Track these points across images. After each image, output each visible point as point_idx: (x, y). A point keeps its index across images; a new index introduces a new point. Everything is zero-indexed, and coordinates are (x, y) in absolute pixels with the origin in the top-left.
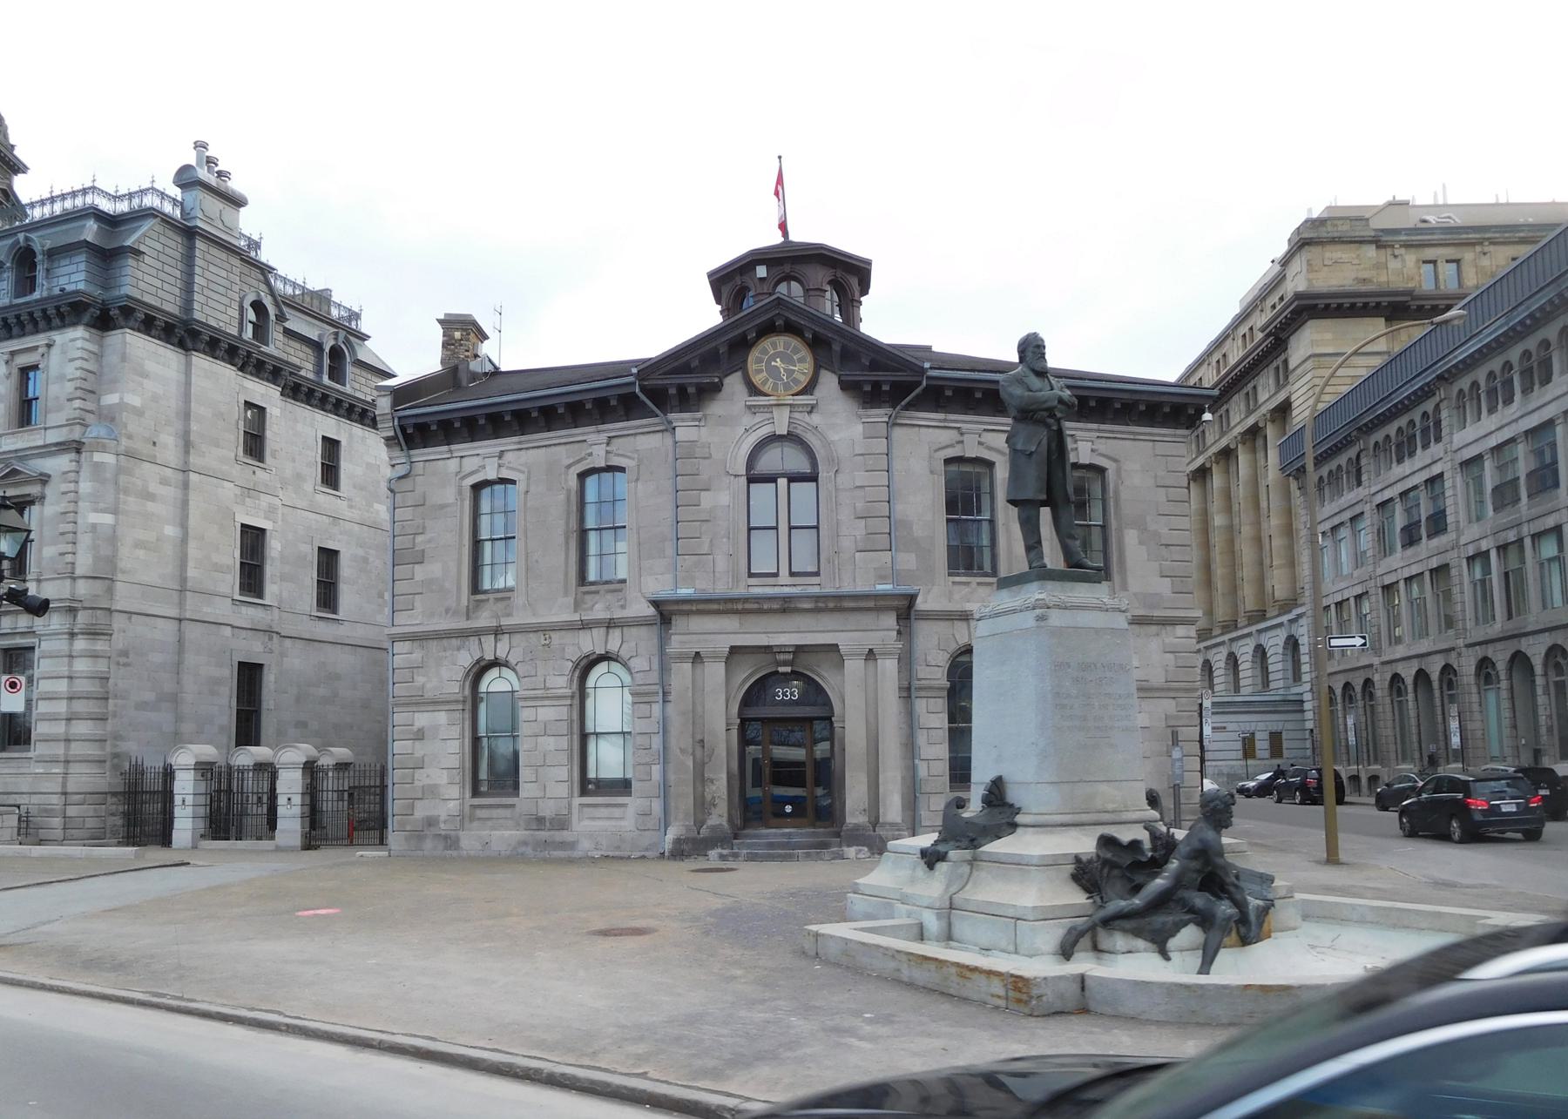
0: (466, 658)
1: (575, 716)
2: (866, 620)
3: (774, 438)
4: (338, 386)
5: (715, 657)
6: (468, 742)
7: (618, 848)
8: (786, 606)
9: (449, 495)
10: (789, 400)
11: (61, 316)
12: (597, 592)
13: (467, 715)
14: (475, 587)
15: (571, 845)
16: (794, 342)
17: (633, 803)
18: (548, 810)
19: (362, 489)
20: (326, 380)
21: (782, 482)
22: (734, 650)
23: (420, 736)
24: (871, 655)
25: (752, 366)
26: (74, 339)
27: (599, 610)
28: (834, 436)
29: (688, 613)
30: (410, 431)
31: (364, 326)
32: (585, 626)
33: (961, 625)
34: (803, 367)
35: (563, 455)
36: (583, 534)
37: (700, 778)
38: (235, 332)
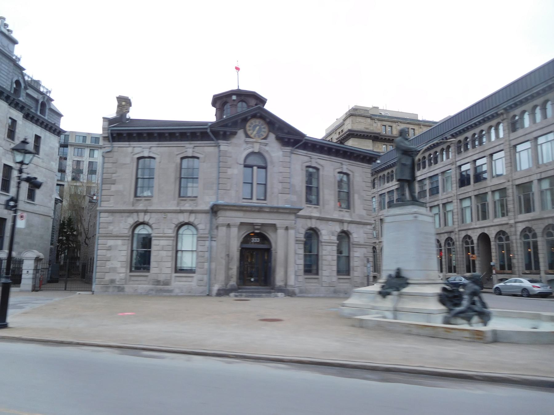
0: (131, 221)
1: (175, 244)
2: (285, 216)
3: (253, 153)
4: (43, 116)
5: (234, 226)
6: (129, 251)
7: (190, 292)
8: (260, 210)
9: (128, 160)
10: (260, 141)
12: (185, 200)
13: (130, 242)
14: (136, 196)
15: (171, 291)
16: (262, 122)
17: (196, 276)
18: (162, 278)
19: (47, 156)
20: (39, 113)
22: (242, 224)
23: (109, 249)
24: (287, 228)
25: (248, 128)
27: (187, 206)
28: (273, 155)
29: (226, 210)
30: (115, 135)
31: (52, 96)
32: (182, 212)
34: (265, 129)
37: (228, 269)
38: (9, 90)
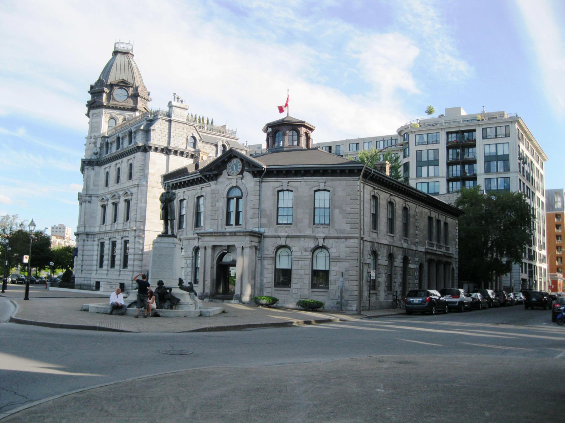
3: (232, 188)
10: (235, 177)
21: (235, 199)
26: (139, 155)
33: (278, 239)
35: (194, 192)
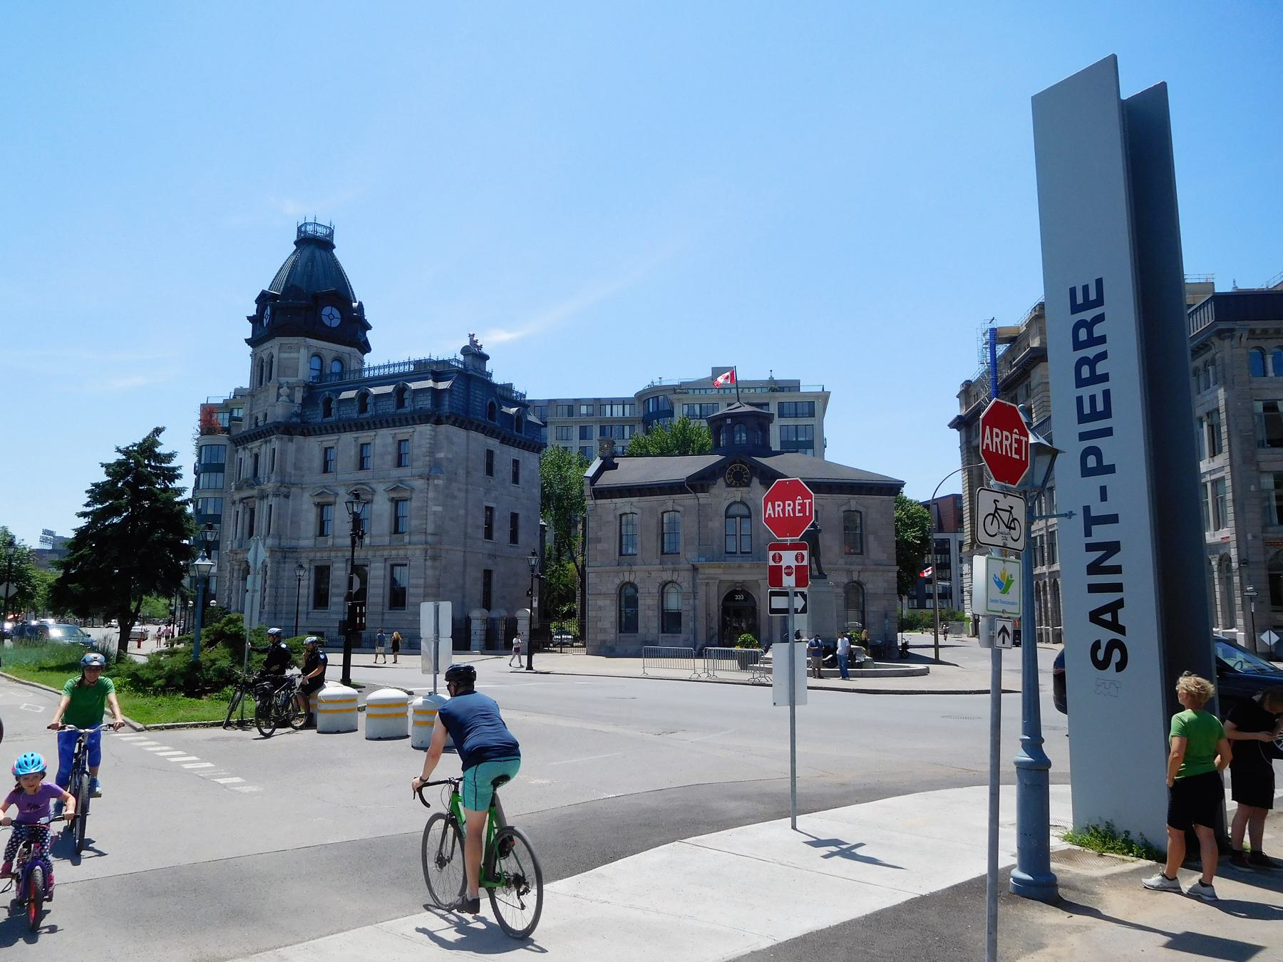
3: (735, 502)
9: (611, 518)
11: (413, 419)
14: (621, 554)
36: (663, 534)
